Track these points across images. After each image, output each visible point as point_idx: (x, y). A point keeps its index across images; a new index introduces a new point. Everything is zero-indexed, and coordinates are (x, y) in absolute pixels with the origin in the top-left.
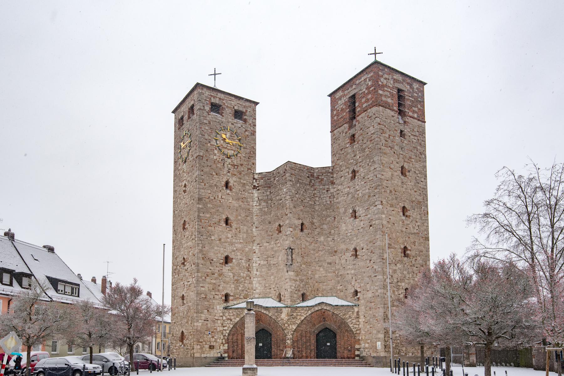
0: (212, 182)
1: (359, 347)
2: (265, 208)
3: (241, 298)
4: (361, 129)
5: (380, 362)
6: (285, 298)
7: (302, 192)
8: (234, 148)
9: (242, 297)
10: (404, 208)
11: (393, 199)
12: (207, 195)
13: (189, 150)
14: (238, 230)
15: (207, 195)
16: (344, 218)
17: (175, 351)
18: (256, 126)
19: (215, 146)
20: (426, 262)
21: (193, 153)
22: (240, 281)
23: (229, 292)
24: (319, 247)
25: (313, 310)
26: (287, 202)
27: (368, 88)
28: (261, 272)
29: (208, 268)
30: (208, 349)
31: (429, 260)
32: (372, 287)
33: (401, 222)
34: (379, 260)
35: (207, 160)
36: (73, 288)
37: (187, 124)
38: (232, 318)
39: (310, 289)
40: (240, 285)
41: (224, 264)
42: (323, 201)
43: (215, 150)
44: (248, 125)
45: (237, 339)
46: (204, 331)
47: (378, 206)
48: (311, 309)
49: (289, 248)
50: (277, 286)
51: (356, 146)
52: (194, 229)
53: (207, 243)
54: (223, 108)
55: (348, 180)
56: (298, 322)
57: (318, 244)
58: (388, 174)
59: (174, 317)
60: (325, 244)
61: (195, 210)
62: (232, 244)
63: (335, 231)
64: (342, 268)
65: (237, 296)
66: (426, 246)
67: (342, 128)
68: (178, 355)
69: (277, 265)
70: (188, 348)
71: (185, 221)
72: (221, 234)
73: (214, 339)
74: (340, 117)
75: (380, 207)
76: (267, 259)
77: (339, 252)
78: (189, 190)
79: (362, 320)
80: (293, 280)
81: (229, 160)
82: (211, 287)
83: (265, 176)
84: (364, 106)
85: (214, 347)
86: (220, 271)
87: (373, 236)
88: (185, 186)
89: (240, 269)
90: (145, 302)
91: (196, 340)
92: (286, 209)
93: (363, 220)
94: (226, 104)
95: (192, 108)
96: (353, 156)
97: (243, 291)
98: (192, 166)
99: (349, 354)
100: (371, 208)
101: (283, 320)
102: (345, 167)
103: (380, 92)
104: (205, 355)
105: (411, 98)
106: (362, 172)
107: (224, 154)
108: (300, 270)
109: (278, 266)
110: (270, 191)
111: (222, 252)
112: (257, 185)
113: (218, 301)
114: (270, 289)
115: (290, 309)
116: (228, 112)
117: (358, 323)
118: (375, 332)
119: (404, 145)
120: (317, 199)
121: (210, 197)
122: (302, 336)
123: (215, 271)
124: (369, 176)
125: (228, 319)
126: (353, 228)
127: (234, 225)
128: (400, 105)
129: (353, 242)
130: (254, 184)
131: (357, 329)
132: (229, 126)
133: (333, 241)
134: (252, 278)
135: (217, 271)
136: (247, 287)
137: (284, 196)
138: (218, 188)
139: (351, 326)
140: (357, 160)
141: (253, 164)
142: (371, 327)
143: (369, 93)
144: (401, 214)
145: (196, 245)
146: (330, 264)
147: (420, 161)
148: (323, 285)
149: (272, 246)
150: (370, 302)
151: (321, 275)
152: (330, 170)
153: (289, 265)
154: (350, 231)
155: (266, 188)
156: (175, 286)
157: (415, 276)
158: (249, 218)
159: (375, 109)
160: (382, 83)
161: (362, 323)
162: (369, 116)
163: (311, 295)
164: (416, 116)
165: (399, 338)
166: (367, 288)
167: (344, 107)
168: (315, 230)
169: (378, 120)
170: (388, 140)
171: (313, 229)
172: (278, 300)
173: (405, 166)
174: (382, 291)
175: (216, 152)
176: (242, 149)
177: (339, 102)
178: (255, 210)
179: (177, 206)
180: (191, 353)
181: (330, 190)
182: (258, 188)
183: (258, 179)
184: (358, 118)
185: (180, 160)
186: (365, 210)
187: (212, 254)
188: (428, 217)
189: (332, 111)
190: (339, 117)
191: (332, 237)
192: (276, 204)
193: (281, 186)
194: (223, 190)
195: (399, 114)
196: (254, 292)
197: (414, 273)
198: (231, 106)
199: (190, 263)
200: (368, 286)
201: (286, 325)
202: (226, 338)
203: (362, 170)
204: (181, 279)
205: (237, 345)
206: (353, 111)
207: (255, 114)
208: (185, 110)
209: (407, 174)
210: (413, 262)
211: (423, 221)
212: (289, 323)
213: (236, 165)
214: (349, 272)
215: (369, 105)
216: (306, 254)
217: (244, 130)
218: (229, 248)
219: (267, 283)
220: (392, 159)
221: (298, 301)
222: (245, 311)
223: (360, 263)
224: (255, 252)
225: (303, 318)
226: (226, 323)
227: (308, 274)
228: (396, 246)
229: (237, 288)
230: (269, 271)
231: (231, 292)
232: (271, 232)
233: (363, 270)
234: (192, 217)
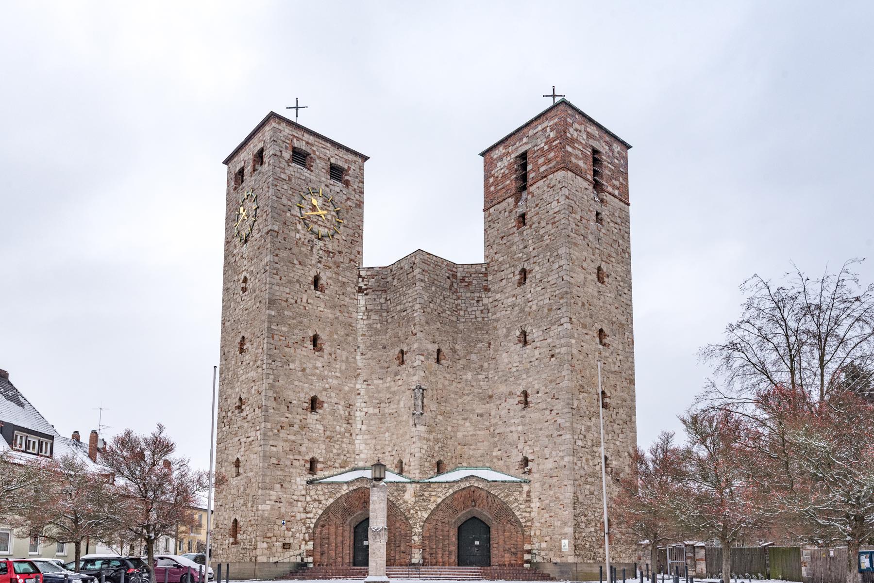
0: (292, 275)
1: (530, 548)
2: (377, 324)
3: (336, 467)
4: (537, 205)
5: (567, 572)
6: (410, 468)
7: (438, 301)
8: (328, 224)
9: (337, 465)
10: (601, 331)
11: (586, 316)
12: (284, 295)
13: (254, 221)
14: (333, 356)
15: (284, 295)
16: (506, 343)
17: (221, 552)
18: (363, 193)
19: (298, 218)
20: (630, 417)
21: (261, 227)
22: (335, 439)
23: (316, 456)
24: (464, 389)
25: (456, 488)
26: (415, 315)
27: (549, 142)
28: (369, 425)
29: (283, 415)
30: (280, 550)
31: (635, 415)
32: (554, 453)
33: (597, 353)
34: (566, 410)
35: (285, 239)
36: (42, 442)
37: (249, 180)
38: (322, 498)
39: (449, 454)
40: (335, 445)
41: (309, 409)
42: (471, 317)
43: (298, 224)
44: (351, 190)
46: (274, 519)
47: (565, 325)
48: (454, 485)
49: (418, 387)
50: (396, 449)
51: (527, 231)
53: (282, 373)
54: (311, 158)
55: (513, 284)
56: (432, 506)
57: (463, 384)
58: (579, 277)
59: (221, 496)
60: (474, 384)
61: (263, 318)
62: (322, 378)
63: (489, 364)
64: (500, 423)
65: (329, 463)
66: (631, 393)
67: (504, 204)
68: (226, 559)
69: (396, 415)
70: (244, 547)
71: (243, 337)
72: (305, 361)
73: (291, 533)
74: (501, 186)
75: (569, 326)
76: (378, 405)
77: (497, 397)
78: (253, 287)
79: (535, 504)
80: (424, 439)
81: (321, 243)
82: (287, 447)
83: (378, 273)
84: (542, 169)
85: (290, 545)
86: (303, 420)
87: (556, 372)
88: (245, 280)
89: (334, 420)
90: (178, 465)
91: (261, 533)
92: (414, 325)
93: (539, 347)
94: (317, 153)
95: (259, 157)
96: (521, 247)
97: (339, 455)
98: (259, 248)
99: (512, 558)
100: (553, 328)
101: (407, 502)
102: (508, 265)
103: (569, 149)
104: (275, 560)
105: (609, 165)
106: (537, 271)
107: (313, 232)
108: (434, 425)
109: (399, 416)
110: (385, 296)
111: (306, 390)
113: (298, 471)
114: (384, 453)
115: (418, 486)
116: (320, 166)
117: (529, 510)
118: (558, 524)
119: (602, 235)
120: (462, 313)
121: (289, 300)
122: (436, 529)
123: (295, 421)
124: (550, 279)
125: (315, 500)
127: (327, 348)
128: (595, 173)
129: (521, 381)
130: (359, 285)
131: (527, 519)
132: (322, 189)
133: (487, 380)
134: (354, 435)
135: (298, 421)
136: (346, 449)
137: (411, 304)
138: (302, 287)
139: (517, 514)
141: (359, 253)
142: (551, 517)
143: (550, 149)
144: (598, 340)
145: (264, 377)
146: (482, 415)
147: (622, 262)
148: (470, 449)
149: (388, 384)
150: (551, 477)
151: (466, 433)
152: (483, 270)
153: (418, 416)
154: (515, 365)
155: (380, 293)
156: (222, 445)
157: (616, 437)
158: (350, 338)
159: (561, 174)
160: (572, 135)
161: (535, 510)
162: (551, 186)
163: (451, 465)
164: (616, 192)
165: (595, 534)
166: (545, 455)
167: (507, 172)
168: (458, 361)
169: (565, 191)
170: (579, 224)
171: (455, 360)
172: (397, 471)
173: (602, 267)
174: (571, 458)
175: (299, 227)
176: (342, 228)
177: (499, 164)
178: (361, 326)
179: (228, 313)
180: (251, 555)
181: (482, 301)
182: (365, 292)
183: (366, 277)
184: (531, 189)
185: (237, 240)
186: (542, 331)
187: (290, 393)
188: (633, 348)
189: (487, 176)
190: (499, 188)
192: (396, 317)
193: (404, 290)
194: (310, 289)
195: (594, 187)
196: (357, 457)
197: (615, 433)
198: (325, 157)
199: (252, 407)
200: (547, 452)
201: (412, 511)
202: (311, 531)
203: (537, 268)
204: (234, 433)
205: (328, 544)
206: (524, 178)
207: (363, 175)
208: (246, 158)
209: (606, 279)
210: (614, 416)
211: (628, 355)
212: (417, 508)
213: (332, 253)
214: (513, 429)
215: (551, 168)
216: (443, 399)
217: (345, 197)
218: (319, 385)
219: (378, 444)
220: (585, 253)
221: (432, 473)
223: (532, 414)
224: (359, 394)
225: (439, 500)
226: (312, 506)
227: (446, 431)
228: (591, 390)
229: (329, 450)
230: (383, 425)
231: (320, 456)
232: (386, 362)
233: (538, 426)
234: (257, 330)
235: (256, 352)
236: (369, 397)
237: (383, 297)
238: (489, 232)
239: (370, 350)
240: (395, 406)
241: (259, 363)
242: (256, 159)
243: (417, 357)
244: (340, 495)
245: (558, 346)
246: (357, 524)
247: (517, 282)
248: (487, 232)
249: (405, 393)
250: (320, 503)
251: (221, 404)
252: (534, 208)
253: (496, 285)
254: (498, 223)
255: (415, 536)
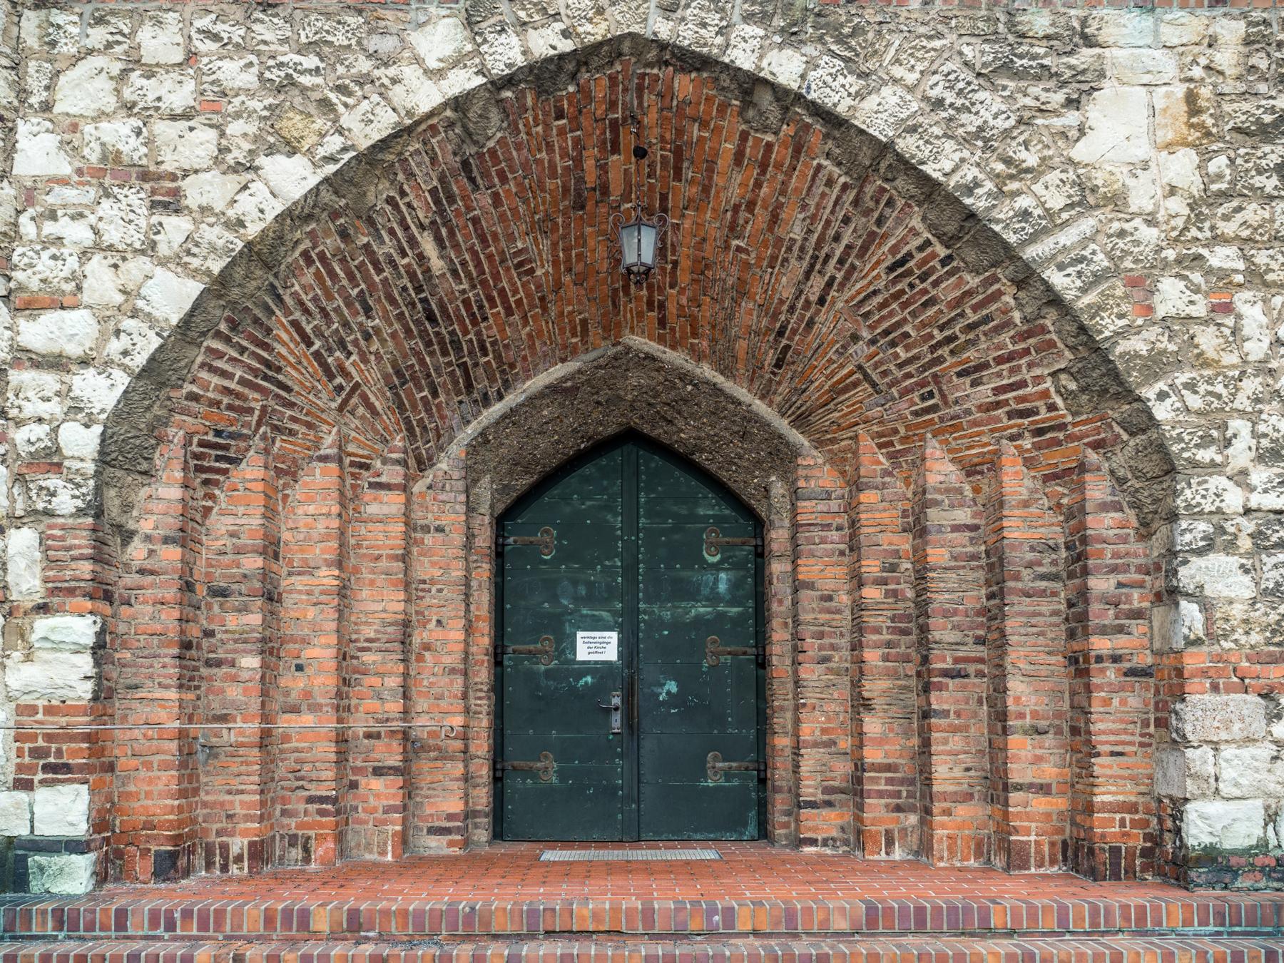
45: (272, 548)
101: (1116, 201)
202: (66, 502)
205: (270, 647)
212: (1222, 257)
222: (415, 37)
226: (78, 233)
244: (385, 123)
246: (524, 482)
250: (170, 203)
255: (1217, 560)
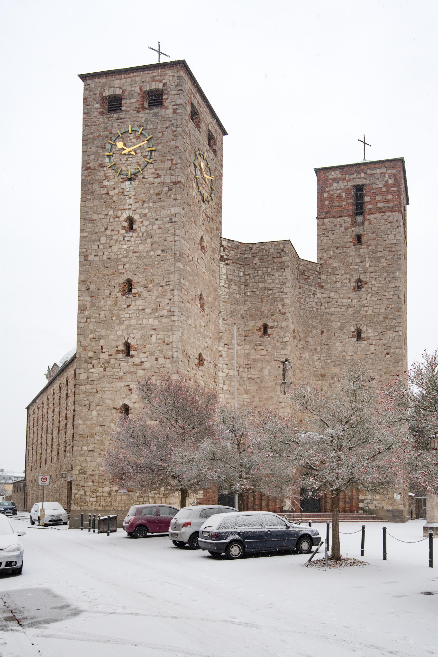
2: (236, 294)
16: (341, 335)
24: (303, 366)
52: (167, 301)
60: (311, 363)
74: (337, 204)
83: (237, 246)
92: (283, 305)
93: (375, 344)
96: (358, 260)
100: (388, 332)
102: (343, 272)
110: (243, 271)
112: (225, 257)
124: (386, 294)
126: (355, 351)
130: (221, 254)
133: (319, 361)
137: (279, 286)
140: (365, 268)
149: (247, 352)
152: (318, 269)
154: (351, 354)
155: (239, 266)
182: (226, 262)
183: (227, 248)
184: (368, 217)
186: (379, 333)
191: (318, 355)
192: (258, 293)
203: (374, 282)
224: (221, 356)
232: (245, 331)
235: (158, 300)
236: (229, 360)
237: (242, 270)
238: (322, 238)
239: (231, 317)
240: (257, 373)
241: (165, 313)
242: (144, 95)
243: (287, 334)
245: (393, 347)
247: (353, 288)
248: (320, 237)
249: (271, 362)
251: (82, 343)
252: (372, 233)
253: (329, 285)
254: (333, 234)
